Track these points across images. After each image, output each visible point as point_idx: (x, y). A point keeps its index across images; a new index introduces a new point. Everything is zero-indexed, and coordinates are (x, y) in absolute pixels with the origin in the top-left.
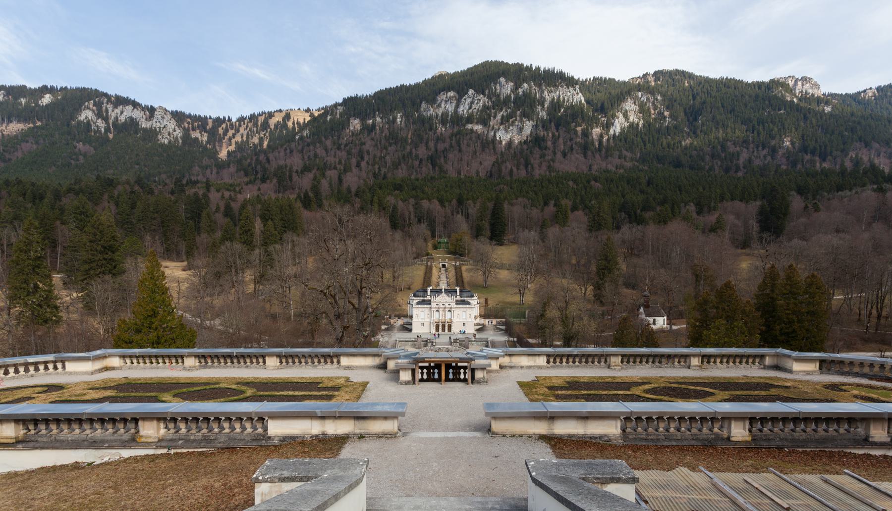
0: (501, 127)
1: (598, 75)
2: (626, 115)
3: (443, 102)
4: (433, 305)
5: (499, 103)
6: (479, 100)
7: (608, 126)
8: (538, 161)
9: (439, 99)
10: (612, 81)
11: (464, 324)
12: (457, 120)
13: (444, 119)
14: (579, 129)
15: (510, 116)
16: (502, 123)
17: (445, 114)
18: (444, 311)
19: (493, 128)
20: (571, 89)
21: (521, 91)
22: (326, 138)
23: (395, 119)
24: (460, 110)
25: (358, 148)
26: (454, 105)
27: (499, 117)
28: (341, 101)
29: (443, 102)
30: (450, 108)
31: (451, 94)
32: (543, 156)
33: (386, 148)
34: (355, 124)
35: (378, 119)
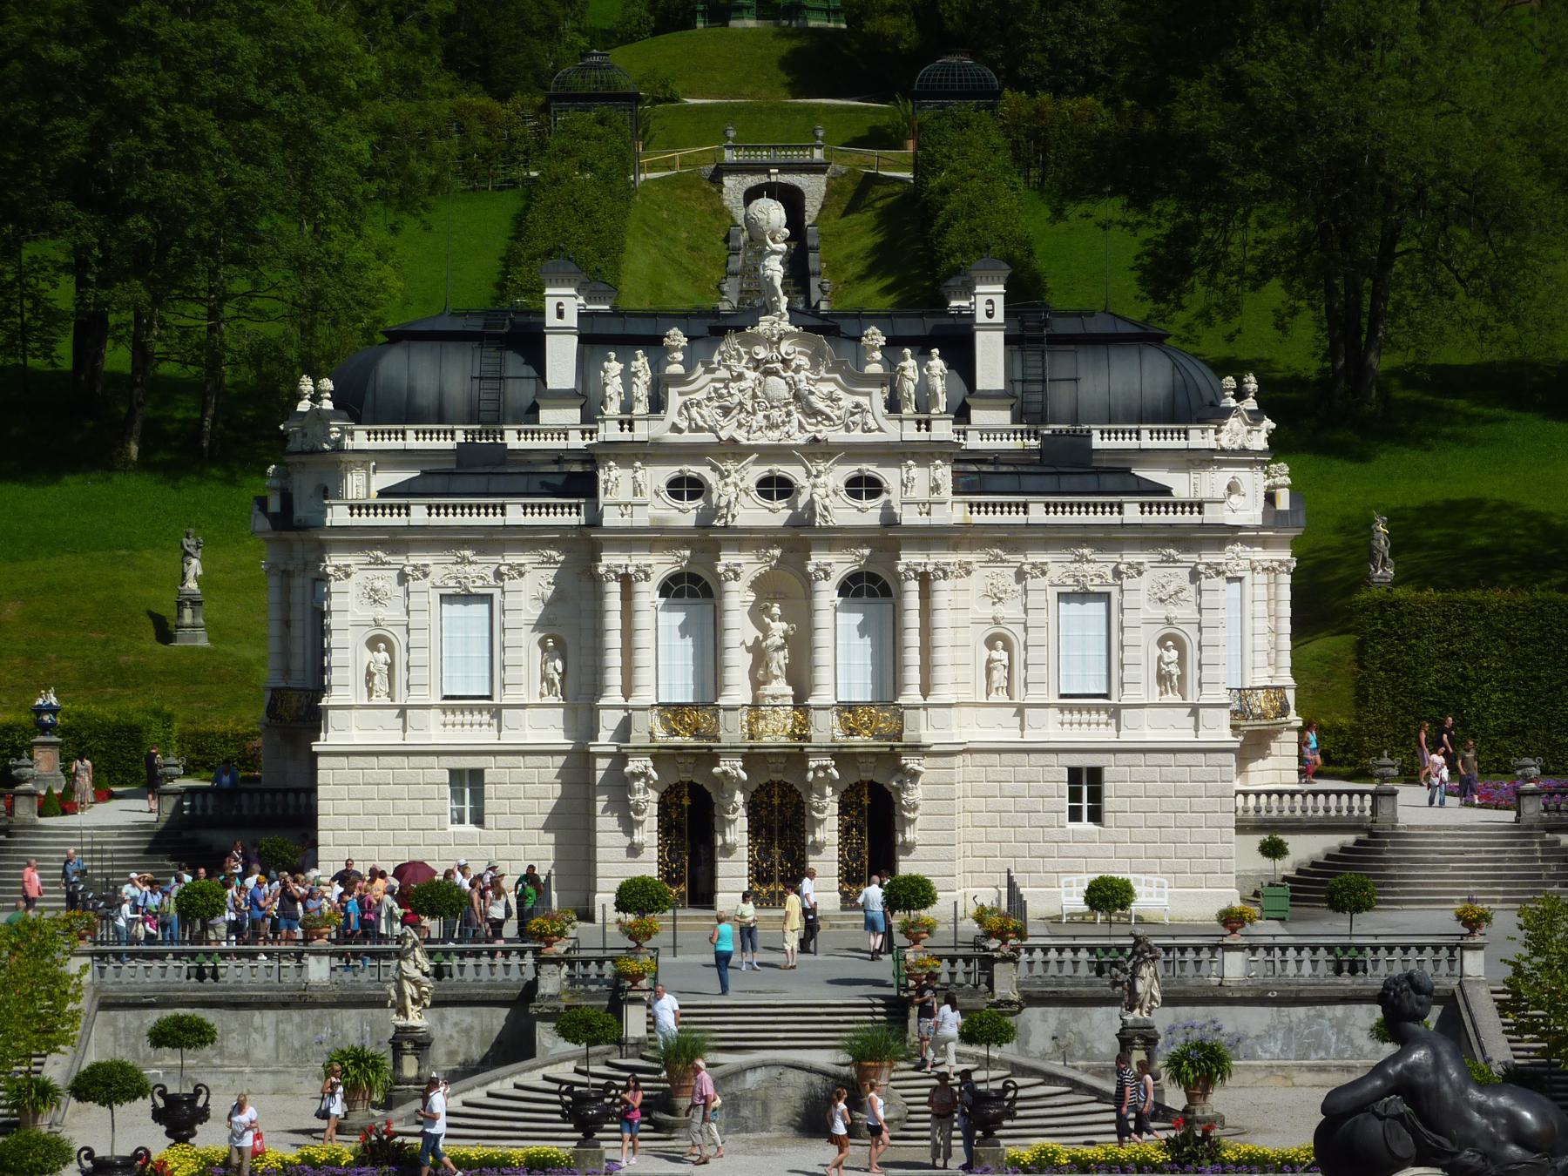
4: (634, 496)
11: (1086, 789)
18: (786, 590)
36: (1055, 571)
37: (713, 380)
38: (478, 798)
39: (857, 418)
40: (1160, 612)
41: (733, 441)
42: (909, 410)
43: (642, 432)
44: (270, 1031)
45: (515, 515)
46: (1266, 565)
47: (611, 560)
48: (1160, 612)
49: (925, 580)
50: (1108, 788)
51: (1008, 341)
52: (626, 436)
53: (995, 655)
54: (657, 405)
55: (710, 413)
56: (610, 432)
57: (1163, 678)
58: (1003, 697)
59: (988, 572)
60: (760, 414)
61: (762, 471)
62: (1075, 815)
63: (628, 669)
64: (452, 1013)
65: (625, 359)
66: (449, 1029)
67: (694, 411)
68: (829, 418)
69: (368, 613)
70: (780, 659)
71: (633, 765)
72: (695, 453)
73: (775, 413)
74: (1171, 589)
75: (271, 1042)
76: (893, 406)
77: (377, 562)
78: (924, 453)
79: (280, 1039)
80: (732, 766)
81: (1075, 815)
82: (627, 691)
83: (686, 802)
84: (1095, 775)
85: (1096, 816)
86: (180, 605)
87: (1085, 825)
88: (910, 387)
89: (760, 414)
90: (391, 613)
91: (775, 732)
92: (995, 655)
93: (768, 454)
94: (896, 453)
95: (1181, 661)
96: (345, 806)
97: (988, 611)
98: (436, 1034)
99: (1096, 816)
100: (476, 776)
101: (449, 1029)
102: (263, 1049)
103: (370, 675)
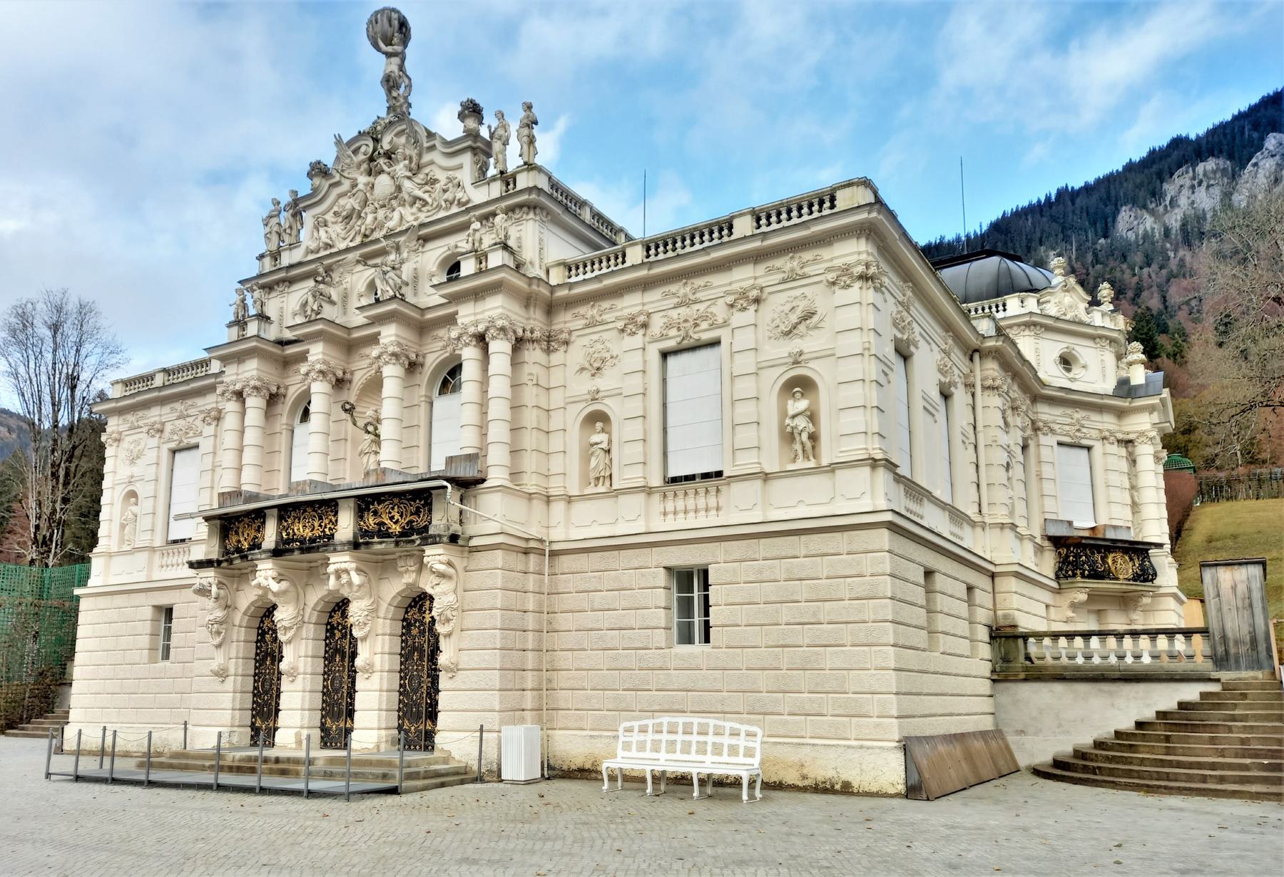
3: (1185, 192)
24: (1240, 199)
29: (1185, 192)
37: (340, 196)
39: (446, 196)
40: (785, 349)
46: (1120, 436)
48: (785, 349)
53: (595, 438)
57: (789, 437)
59: (585, 341)
60: (370, 218)
67: (322, 231)
68: (426, 203)
73: (381, 213)
74: (794, 318)
87: (698, 648)
89: (370, 218)
92: (595, 438)
97: (583, 385)
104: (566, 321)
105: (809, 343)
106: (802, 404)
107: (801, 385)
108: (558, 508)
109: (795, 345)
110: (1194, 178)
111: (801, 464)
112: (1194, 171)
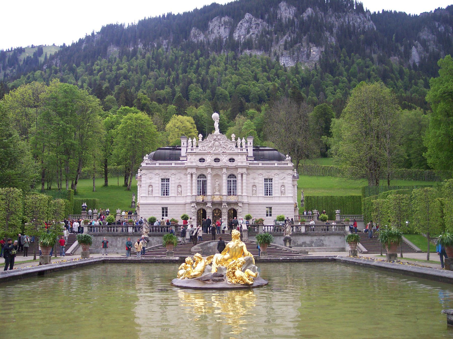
0: (284, 52)
1: (388, 8)
2: (424, 43)
5: (281, 28)
6: (258, 24)
7: (407, 55)
8: (331, 88)
9: (211, 25)
10: (402, 15)
12: (234, 46)
13: (218, 45)
14: (375, 56)
15: (295, 42)
16: (285, 49)
17: (219, 40)
19: (275, 54)
20: (361, 15)
21: (305, 15)
22: (78, 65)
23: (159, 46)
24: (236, 36)
25: (114, 73)
26: (227, 30)
27: (282, 42)
28: (98, 29)
29: (217, 28)
30: (224, 33)
31: (226, 19)
32: (336, 83)
33: (147, 73)
34: (114, 50)
35: (140, 46)
36: (264, 174)
38: (167, 212)
40: (281, 181)
41: (210, 152)
42: (239, 147)
43: (194, 151)
44: (121, 241)
45: (173, 165)
47: (189, 171)
49: (242, 175)
50: (272, 211)
51: (253, 150)
52: (192, 151)
54: (197, 146)
55: (207, 148)
56: (189, 151)
57: (281, 192)
58: (255, 195)
61: (215, 157)
62: (267, 215)
63: (192, 190)
64: (156, 238)
65: (192, 139)
66: (155, 241)
69: (149, 181)
70: (217, 188)
71: (193, 205)
72: (204, 154)
73: (217, 148)
75: (121, 243)
76: (236, 146)
77: (150, 172)
78: (242, 154)
79: (123, 243)
80: (209, 205)
81: (267, 215)
82: (192, 193)
83: (202, 212)
84: (271, 208)
85: (271, 215)
86: (132, 203)
87: (269, 217)
88: (239, 144)
90: (152, 181)
91: (217, 199)
93: (216, 154)
94: (237, 154)
95: (284, 190)
96: (144, 213)
97: (252, 181)
98: (152, 242)
99: (271, 215)
100: (167, 208)
101: (155, 241)
102: (119, 245)
103: (149, 191)
104: (250, 171)
105: (285, 181)
106: (283, 188)
107: (283, 186)
108: (249, 198)
109: (283, 181)
110: (220, 23)
111: (282, 196)
112: (220, 20)
